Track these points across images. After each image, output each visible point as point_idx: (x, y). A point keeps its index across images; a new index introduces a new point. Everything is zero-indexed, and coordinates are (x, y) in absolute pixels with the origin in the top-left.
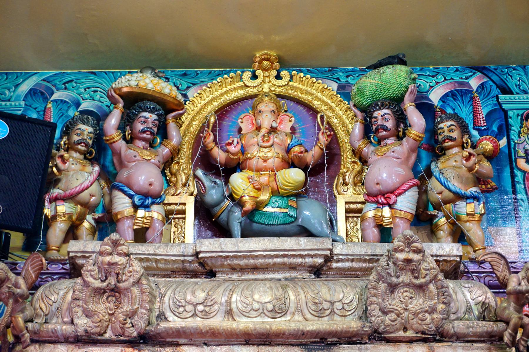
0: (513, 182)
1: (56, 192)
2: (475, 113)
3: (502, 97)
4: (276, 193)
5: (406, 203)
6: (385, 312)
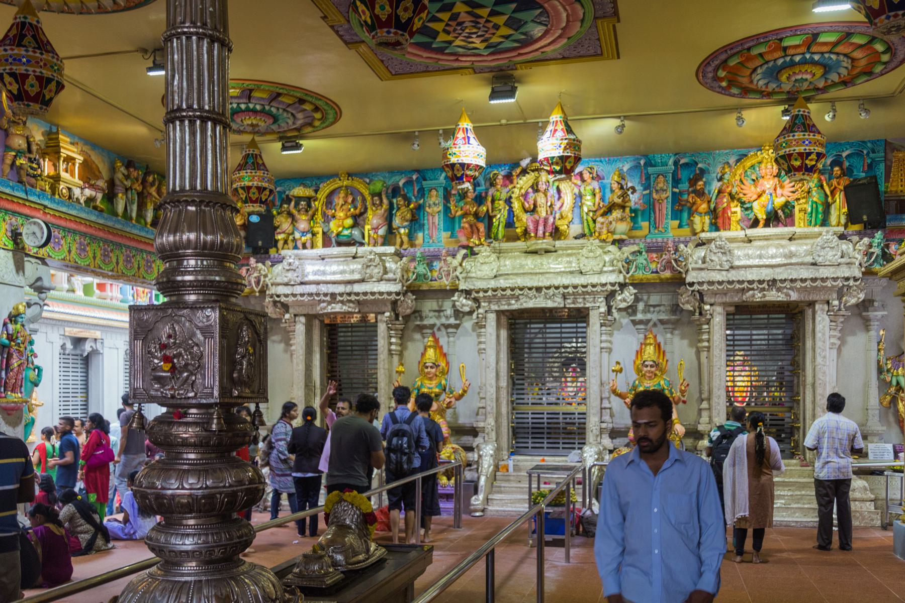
1: (278, 230)
5: (382, 232)
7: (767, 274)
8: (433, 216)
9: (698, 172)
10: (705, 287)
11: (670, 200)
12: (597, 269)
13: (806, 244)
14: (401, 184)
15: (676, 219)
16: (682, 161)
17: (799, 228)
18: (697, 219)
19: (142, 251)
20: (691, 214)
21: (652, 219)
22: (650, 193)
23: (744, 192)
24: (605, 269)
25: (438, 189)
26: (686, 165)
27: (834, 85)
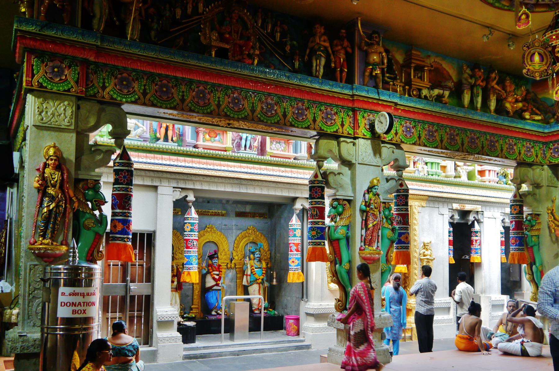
19: (485, 133)
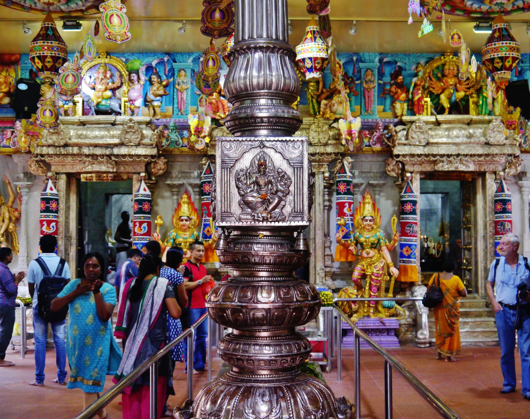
0: (174, 92)
1: (42, 98)
2: (165, 69)
3: (174, 64)
4: (103, 98)
6: (125, 138)
7: (453, 150)
8: (182, 92)
9: (397, 69)
10: (408, 158)
11: (376, 89)
12: (323, 141)
13: (481, 128)
14: (154, 64)
15: (381, 104)
16: (385, 60)
17: (473, 116)
18: (398, 105)
20: (393, 102)
21: (363, 104)
22: (361, 83)
23: (434, 86)
24: (330, 142)
25: (186, 70)
26: (388, 63)
27: (519, 9)
